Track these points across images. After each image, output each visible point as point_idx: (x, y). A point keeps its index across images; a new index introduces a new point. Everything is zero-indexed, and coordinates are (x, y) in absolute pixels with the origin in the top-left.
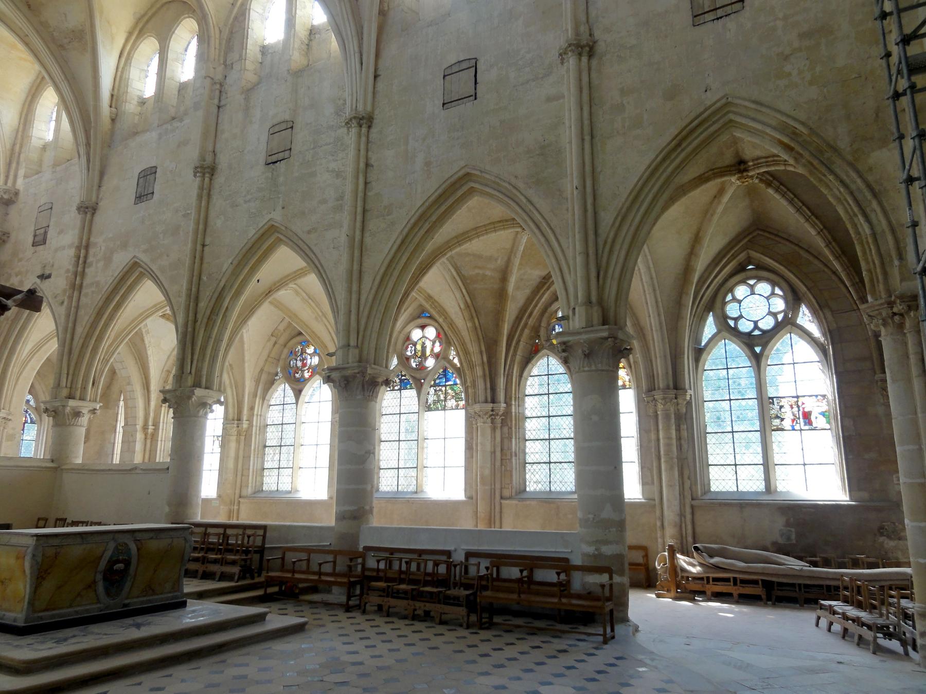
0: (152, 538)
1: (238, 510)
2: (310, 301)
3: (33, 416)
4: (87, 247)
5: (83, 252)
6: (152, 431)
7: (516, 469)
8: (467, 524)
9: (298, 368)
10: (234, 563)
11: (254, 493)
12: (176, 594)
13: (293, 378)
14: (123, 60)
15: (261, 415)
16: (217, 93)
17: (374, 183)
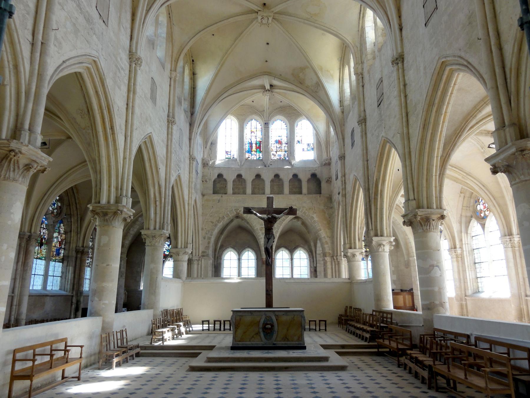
0: (284, 315)
1: (466, 304)
2: (454, 169)
4: (345, 176)
5: (343, 178)
8: (511, 318)
9: (481, 210)
10: (367, 332)
11: (474, 293)
12: (300, 342)
14: (341, 82)
16: (361, 79)
17: (409, 94)
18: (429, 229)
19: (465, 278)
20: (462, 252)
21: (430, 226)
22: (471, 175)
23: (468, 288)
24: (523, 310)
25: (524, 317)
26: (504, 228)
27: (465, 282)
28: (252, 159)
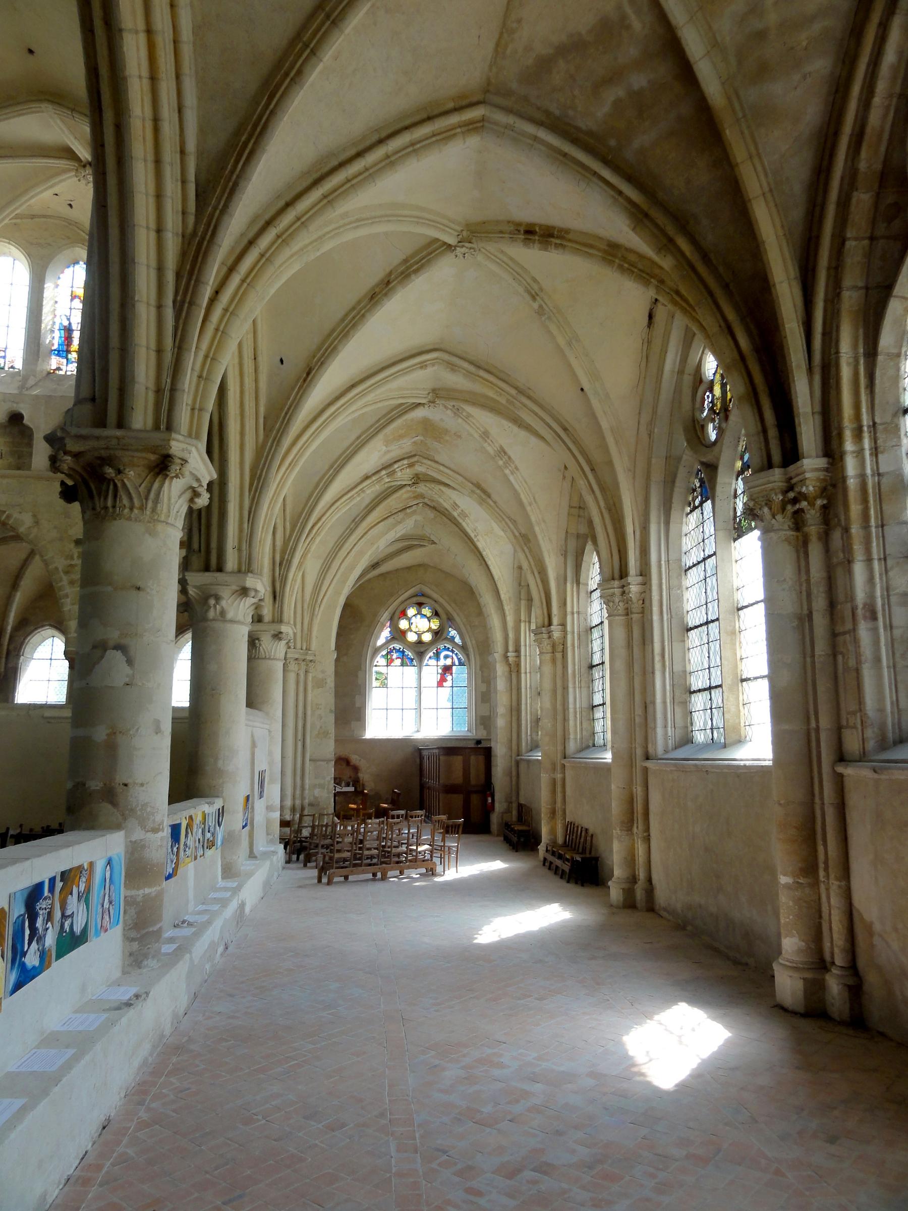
2: (482, 373)
3: (460, 656)
6: (514, 659)
7: (877, 660)
15: (578, 613)
18: (114, 507)
21: (115, 496)
22: (532, 394)
28: (69, 373)
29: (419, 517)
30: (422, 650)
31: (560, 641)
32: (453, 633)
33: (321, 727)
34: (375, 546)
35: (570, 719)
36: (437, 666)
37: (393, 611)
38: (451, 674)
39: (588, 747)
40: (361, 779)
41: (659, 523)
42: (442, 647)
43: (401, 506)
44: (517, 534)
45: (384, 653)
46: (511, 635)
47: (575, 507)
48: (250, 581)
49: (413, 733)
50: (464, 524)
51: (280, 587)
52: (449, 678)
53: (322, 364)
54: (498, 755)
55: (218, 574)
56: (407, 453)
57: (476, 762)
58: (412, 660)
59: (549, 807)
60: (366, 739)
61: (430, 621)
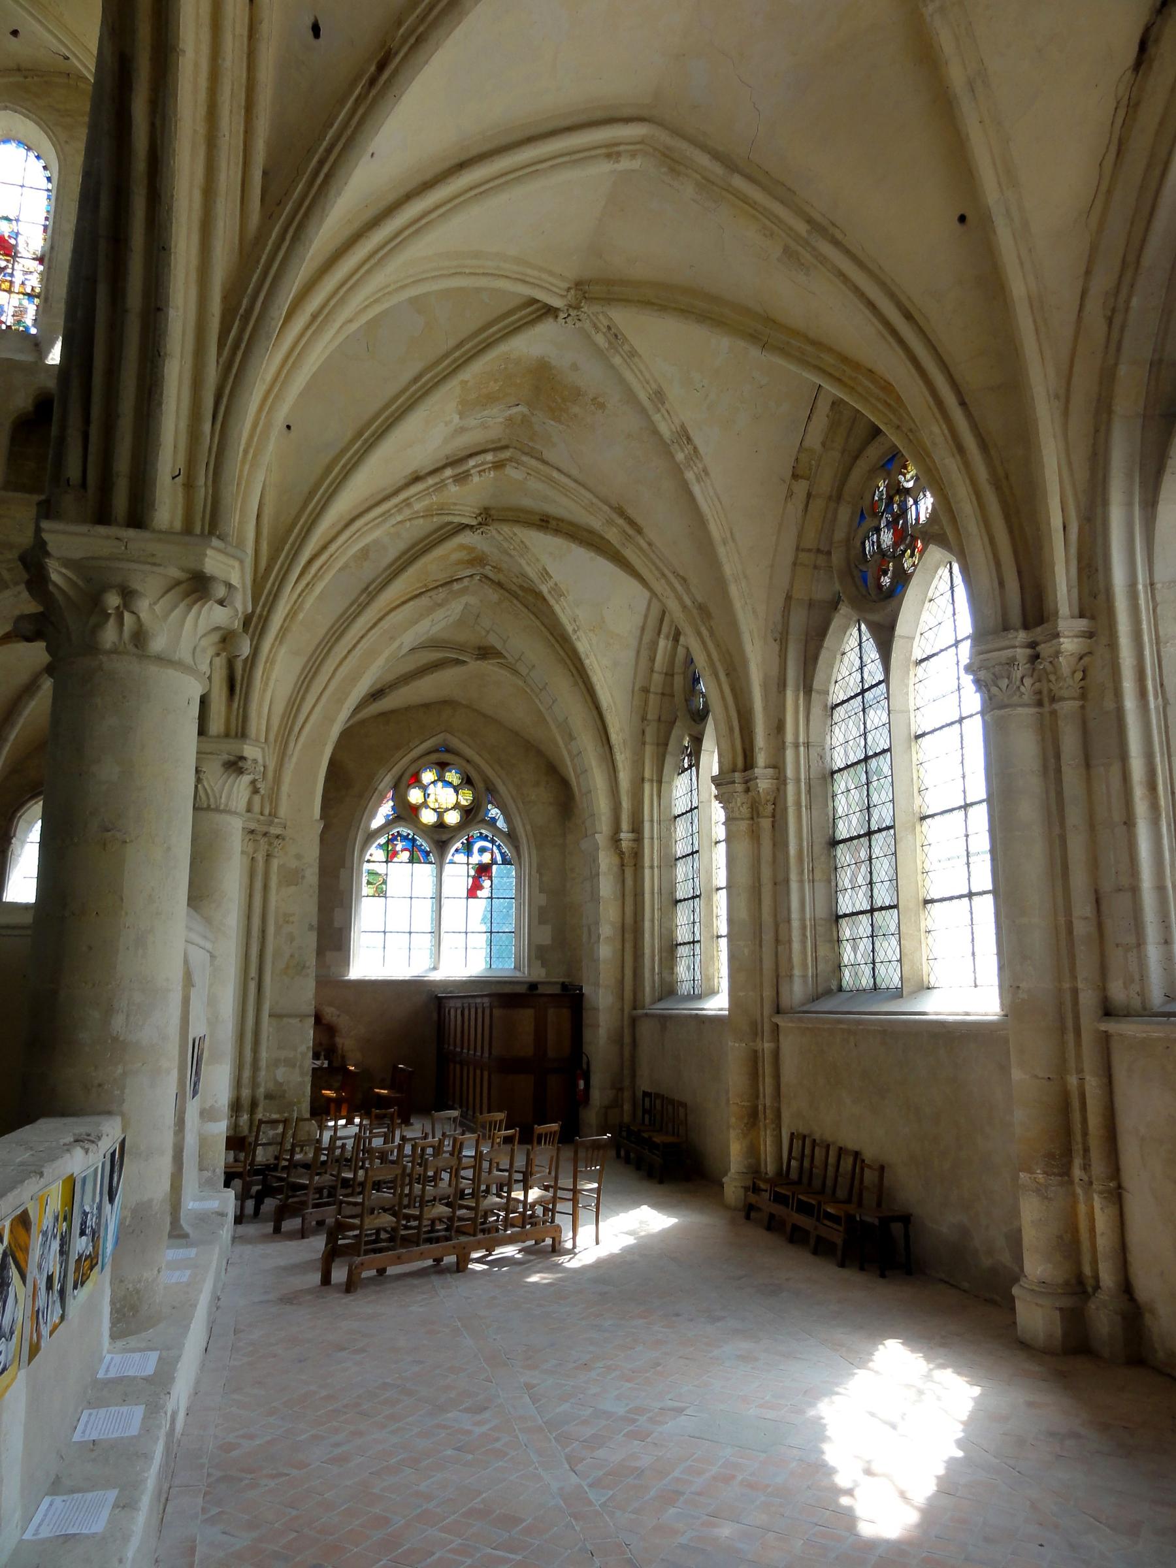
1: (776, 1054)
2: (738, 182)
3: (505, 849)
6: (631, 844)
9: (882, 553)
11: (816, 998)
13: (873, 592)
15: (807, 745)
19: (781, 919)
20: (778, 789)
22: (839, 236)
23: (792, 968)
24: (1076, 1103)
25: (1086, 1150)
26: (1001, 584)
27: (780, 941)
29: (471, 600)
30: (444, 837)
31: (768, 797)
32: (494, 812)
33: (292, 956)
34: (396, 644)
35: (794, 939)
36: (468, 864)
37: (400, 773)
38: (490, 878)
39: (828, 993)
40: (340, 1046)
41: (1129, 504)
42: (476, 833)
43: (443, 577)
44: (688, 602)
45: (382, 840)
46: (626, 804)
47: (809, 550)
48: (215, 563)
49: (426, 971)
50: (557, 608)
51: (244, 670)
52: (486, 883)
53: (419, 40)
54: (601, 1008)
55: (131, 533)
56: (493, 442)
57: (556, 1017)
58: (427, 854)
59: (746, 1104)
60: (350, 981)
61: (457, 792)
